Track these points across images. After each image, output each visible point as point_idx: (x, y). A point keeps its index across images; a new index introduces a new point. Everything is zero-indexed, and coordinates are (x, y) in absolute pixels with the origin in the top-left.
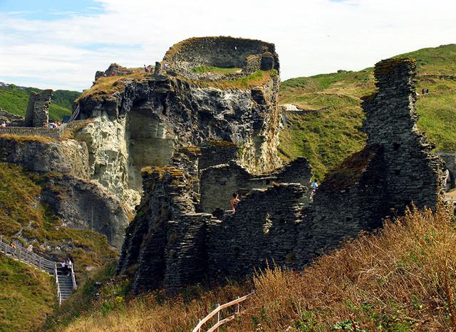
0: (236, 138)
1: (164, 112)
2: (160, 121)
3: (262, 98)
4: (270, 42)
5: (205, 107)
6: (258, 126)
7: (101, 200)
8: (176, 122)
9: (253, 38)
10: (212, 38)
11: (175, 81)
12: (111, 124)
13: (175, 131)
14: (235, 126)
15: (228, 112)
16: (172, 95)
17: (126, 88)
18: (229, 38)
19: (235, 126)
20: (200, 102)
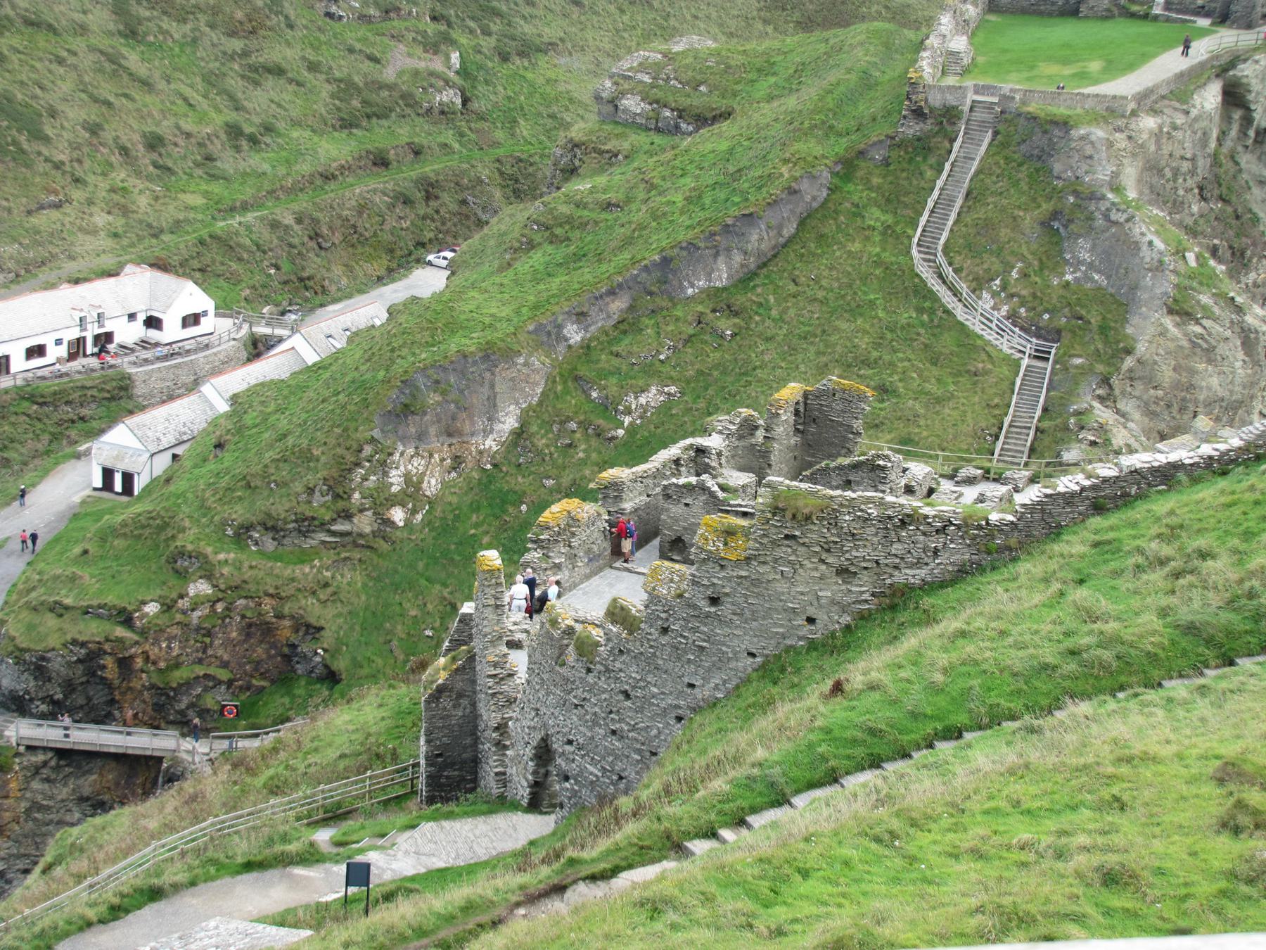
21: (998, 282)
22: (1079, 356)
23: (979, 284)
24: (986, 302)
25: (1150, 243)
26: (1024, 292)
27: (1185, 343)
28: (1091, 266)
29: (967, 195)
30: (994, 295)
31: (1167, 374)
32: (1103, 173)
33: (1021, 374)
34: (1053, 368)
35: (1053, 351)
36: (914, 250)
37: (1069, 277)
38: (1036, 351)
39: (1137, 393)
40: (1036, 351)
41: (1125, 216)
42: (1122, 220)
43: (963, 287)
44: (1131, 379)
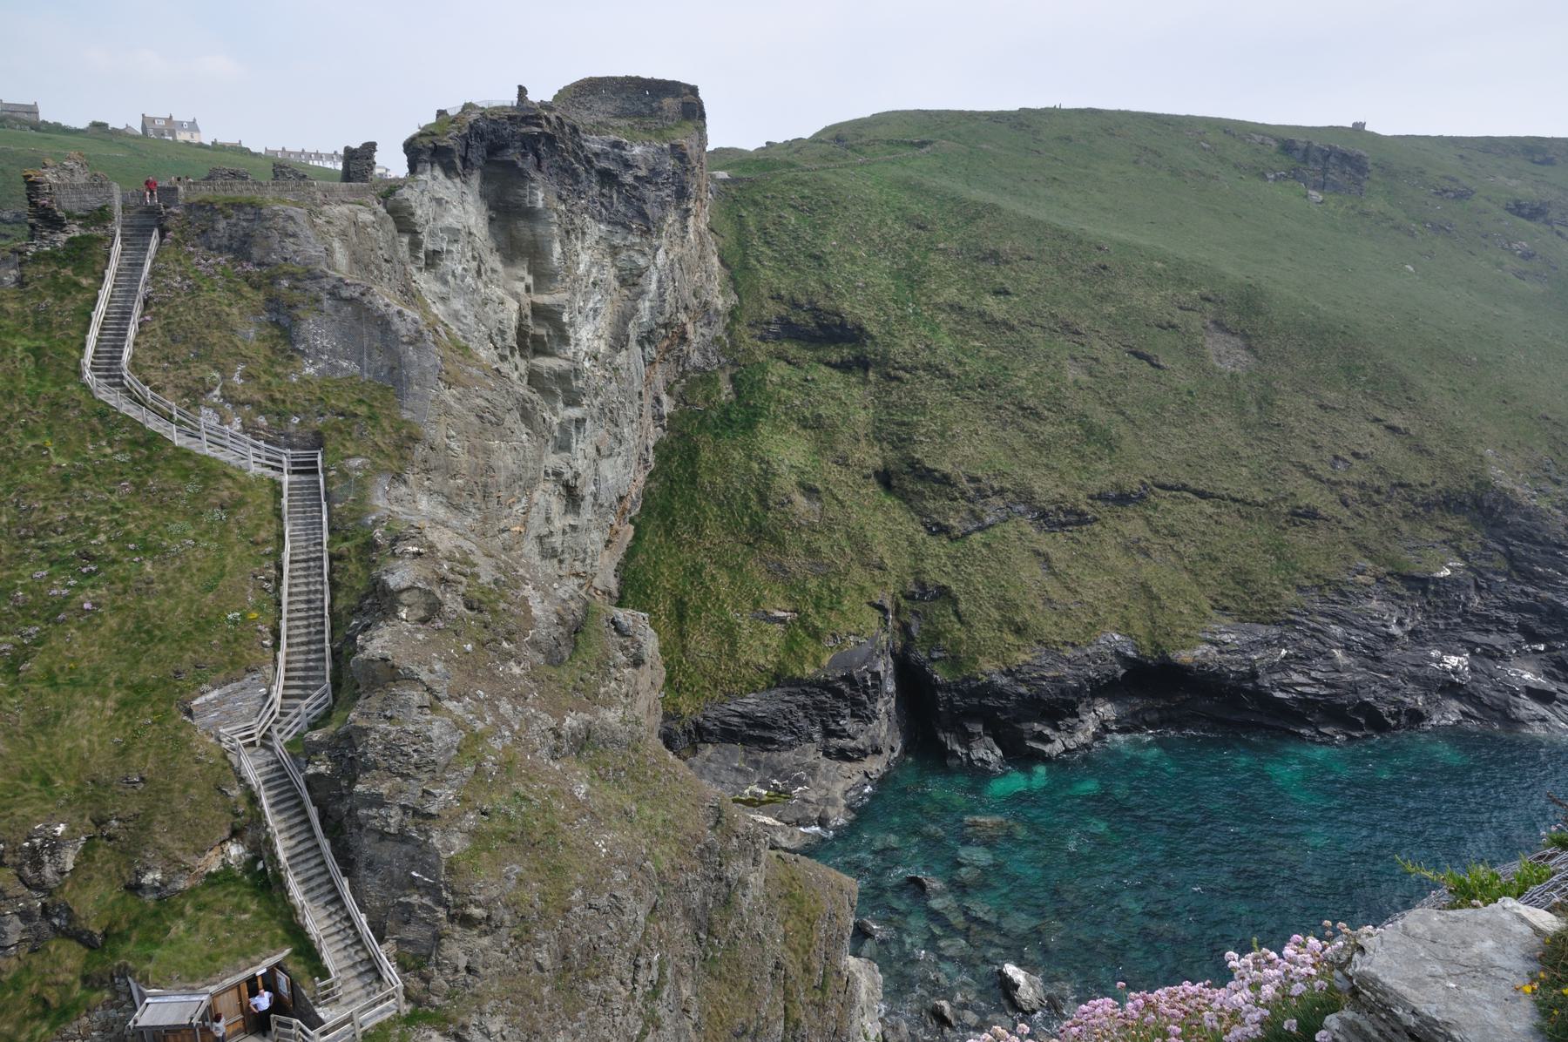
0: (652, 211)
1: (539, 167)
2: (532, 180)
3: (685, 155)
4: (692, 83)
5: (604, 164)
6: (682, 194)
7: (382, 317)
8: (561, 184)
9: (669, 78)
10: (614, 79)
11: (553, 119)
12: (449, 183)
13: (560, 197)
14: (650, 193)
15: (640, 173)
16: (550, 139)
17: (471, 126)
18: (638, 78)
19: (650, 193)
20: (596, 155)
21: (217, 392)
22: (357, 455)
23: (194, 395)
24: (207, 418)
25: (399, 312)
26: (258, 397)
27: (473, 418)
28: (333, 352)
29: (146, 303)
30: (215, 408)
31: (463, 460)
32: (313, 250)
33: (286, 493)
34: (326, 479)
35: (319, 458)
36: (88, 375)
37: (310, 371)
38: (295, 464)
39: (436, 488)
40: (295, 464)
41: (359, 290)
42: (356, 295)
43: (171, 404)
44: (427, 471)
